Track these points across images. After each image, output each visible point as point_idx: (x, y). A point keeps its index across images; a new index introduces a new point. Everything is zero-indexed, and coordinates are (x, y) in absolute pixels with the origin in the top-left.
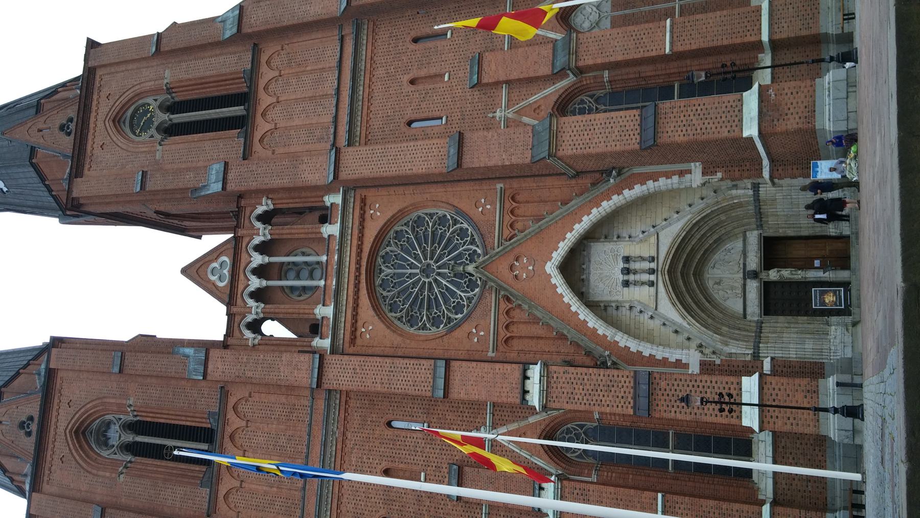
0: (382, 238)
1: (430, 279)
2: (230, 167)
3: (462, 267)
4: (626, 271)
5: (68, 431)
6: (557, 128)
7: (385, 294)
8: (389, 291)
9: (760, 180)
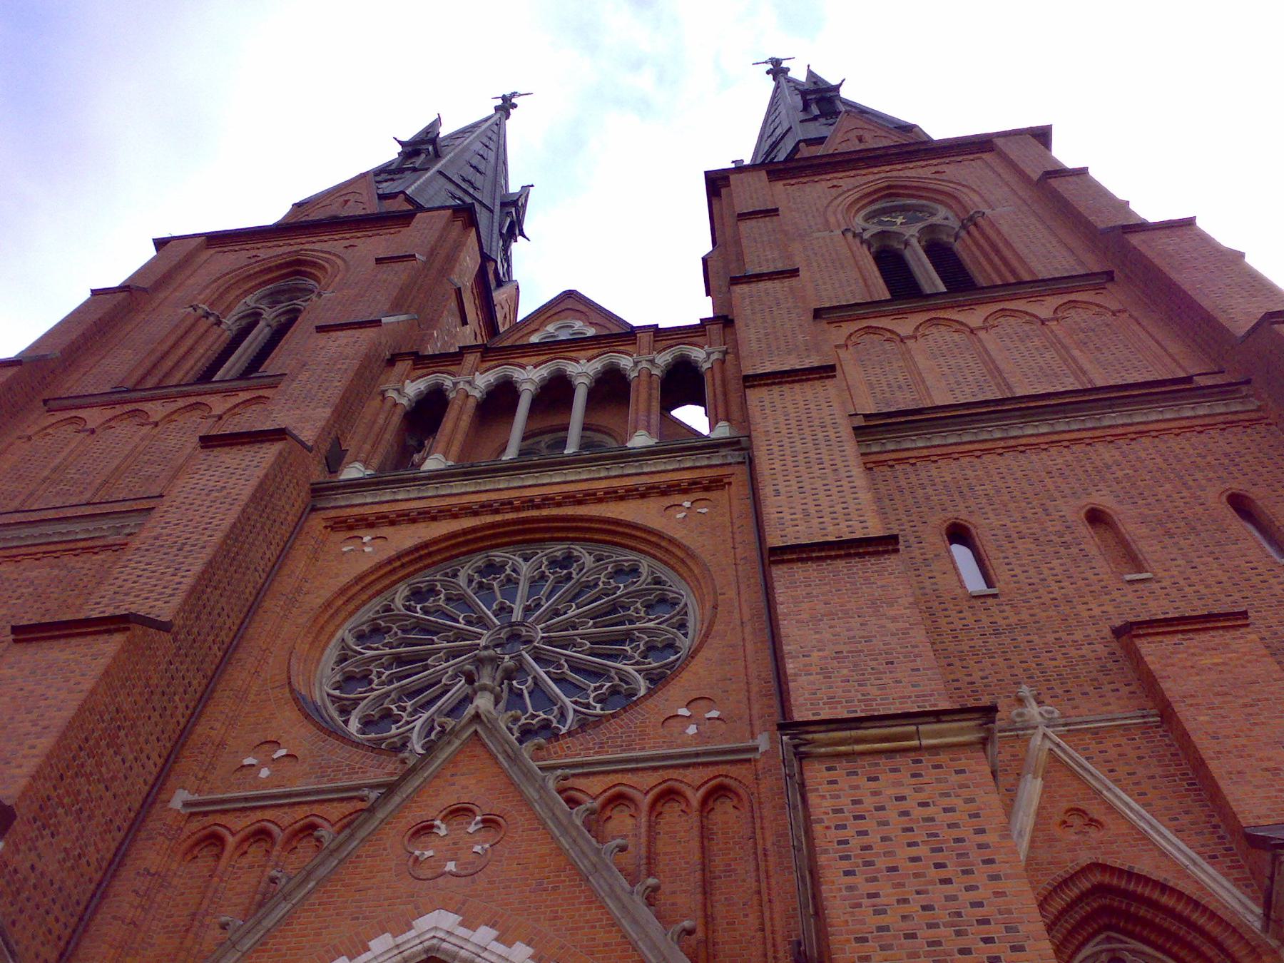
0: (617, 539)
6: (934, 749)
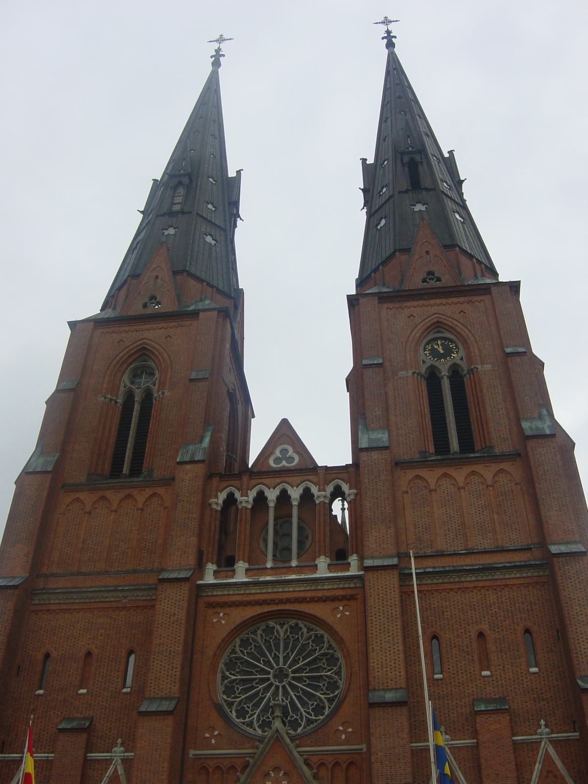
1: (272, 680)
2: (383, 452)
3: (279, 714)
5: (144, 340)
7: (259, 632)
8: (262, 635)
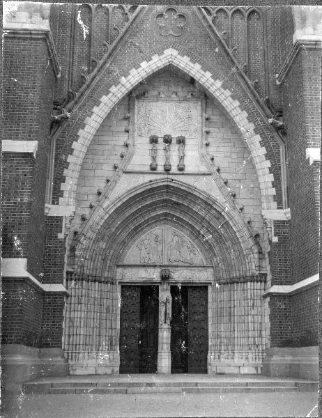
4: (168, 140)
9: (269, 283)
